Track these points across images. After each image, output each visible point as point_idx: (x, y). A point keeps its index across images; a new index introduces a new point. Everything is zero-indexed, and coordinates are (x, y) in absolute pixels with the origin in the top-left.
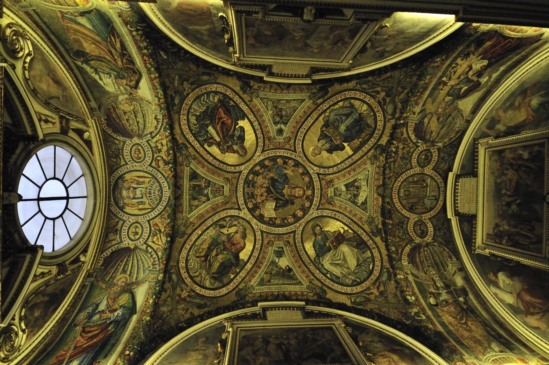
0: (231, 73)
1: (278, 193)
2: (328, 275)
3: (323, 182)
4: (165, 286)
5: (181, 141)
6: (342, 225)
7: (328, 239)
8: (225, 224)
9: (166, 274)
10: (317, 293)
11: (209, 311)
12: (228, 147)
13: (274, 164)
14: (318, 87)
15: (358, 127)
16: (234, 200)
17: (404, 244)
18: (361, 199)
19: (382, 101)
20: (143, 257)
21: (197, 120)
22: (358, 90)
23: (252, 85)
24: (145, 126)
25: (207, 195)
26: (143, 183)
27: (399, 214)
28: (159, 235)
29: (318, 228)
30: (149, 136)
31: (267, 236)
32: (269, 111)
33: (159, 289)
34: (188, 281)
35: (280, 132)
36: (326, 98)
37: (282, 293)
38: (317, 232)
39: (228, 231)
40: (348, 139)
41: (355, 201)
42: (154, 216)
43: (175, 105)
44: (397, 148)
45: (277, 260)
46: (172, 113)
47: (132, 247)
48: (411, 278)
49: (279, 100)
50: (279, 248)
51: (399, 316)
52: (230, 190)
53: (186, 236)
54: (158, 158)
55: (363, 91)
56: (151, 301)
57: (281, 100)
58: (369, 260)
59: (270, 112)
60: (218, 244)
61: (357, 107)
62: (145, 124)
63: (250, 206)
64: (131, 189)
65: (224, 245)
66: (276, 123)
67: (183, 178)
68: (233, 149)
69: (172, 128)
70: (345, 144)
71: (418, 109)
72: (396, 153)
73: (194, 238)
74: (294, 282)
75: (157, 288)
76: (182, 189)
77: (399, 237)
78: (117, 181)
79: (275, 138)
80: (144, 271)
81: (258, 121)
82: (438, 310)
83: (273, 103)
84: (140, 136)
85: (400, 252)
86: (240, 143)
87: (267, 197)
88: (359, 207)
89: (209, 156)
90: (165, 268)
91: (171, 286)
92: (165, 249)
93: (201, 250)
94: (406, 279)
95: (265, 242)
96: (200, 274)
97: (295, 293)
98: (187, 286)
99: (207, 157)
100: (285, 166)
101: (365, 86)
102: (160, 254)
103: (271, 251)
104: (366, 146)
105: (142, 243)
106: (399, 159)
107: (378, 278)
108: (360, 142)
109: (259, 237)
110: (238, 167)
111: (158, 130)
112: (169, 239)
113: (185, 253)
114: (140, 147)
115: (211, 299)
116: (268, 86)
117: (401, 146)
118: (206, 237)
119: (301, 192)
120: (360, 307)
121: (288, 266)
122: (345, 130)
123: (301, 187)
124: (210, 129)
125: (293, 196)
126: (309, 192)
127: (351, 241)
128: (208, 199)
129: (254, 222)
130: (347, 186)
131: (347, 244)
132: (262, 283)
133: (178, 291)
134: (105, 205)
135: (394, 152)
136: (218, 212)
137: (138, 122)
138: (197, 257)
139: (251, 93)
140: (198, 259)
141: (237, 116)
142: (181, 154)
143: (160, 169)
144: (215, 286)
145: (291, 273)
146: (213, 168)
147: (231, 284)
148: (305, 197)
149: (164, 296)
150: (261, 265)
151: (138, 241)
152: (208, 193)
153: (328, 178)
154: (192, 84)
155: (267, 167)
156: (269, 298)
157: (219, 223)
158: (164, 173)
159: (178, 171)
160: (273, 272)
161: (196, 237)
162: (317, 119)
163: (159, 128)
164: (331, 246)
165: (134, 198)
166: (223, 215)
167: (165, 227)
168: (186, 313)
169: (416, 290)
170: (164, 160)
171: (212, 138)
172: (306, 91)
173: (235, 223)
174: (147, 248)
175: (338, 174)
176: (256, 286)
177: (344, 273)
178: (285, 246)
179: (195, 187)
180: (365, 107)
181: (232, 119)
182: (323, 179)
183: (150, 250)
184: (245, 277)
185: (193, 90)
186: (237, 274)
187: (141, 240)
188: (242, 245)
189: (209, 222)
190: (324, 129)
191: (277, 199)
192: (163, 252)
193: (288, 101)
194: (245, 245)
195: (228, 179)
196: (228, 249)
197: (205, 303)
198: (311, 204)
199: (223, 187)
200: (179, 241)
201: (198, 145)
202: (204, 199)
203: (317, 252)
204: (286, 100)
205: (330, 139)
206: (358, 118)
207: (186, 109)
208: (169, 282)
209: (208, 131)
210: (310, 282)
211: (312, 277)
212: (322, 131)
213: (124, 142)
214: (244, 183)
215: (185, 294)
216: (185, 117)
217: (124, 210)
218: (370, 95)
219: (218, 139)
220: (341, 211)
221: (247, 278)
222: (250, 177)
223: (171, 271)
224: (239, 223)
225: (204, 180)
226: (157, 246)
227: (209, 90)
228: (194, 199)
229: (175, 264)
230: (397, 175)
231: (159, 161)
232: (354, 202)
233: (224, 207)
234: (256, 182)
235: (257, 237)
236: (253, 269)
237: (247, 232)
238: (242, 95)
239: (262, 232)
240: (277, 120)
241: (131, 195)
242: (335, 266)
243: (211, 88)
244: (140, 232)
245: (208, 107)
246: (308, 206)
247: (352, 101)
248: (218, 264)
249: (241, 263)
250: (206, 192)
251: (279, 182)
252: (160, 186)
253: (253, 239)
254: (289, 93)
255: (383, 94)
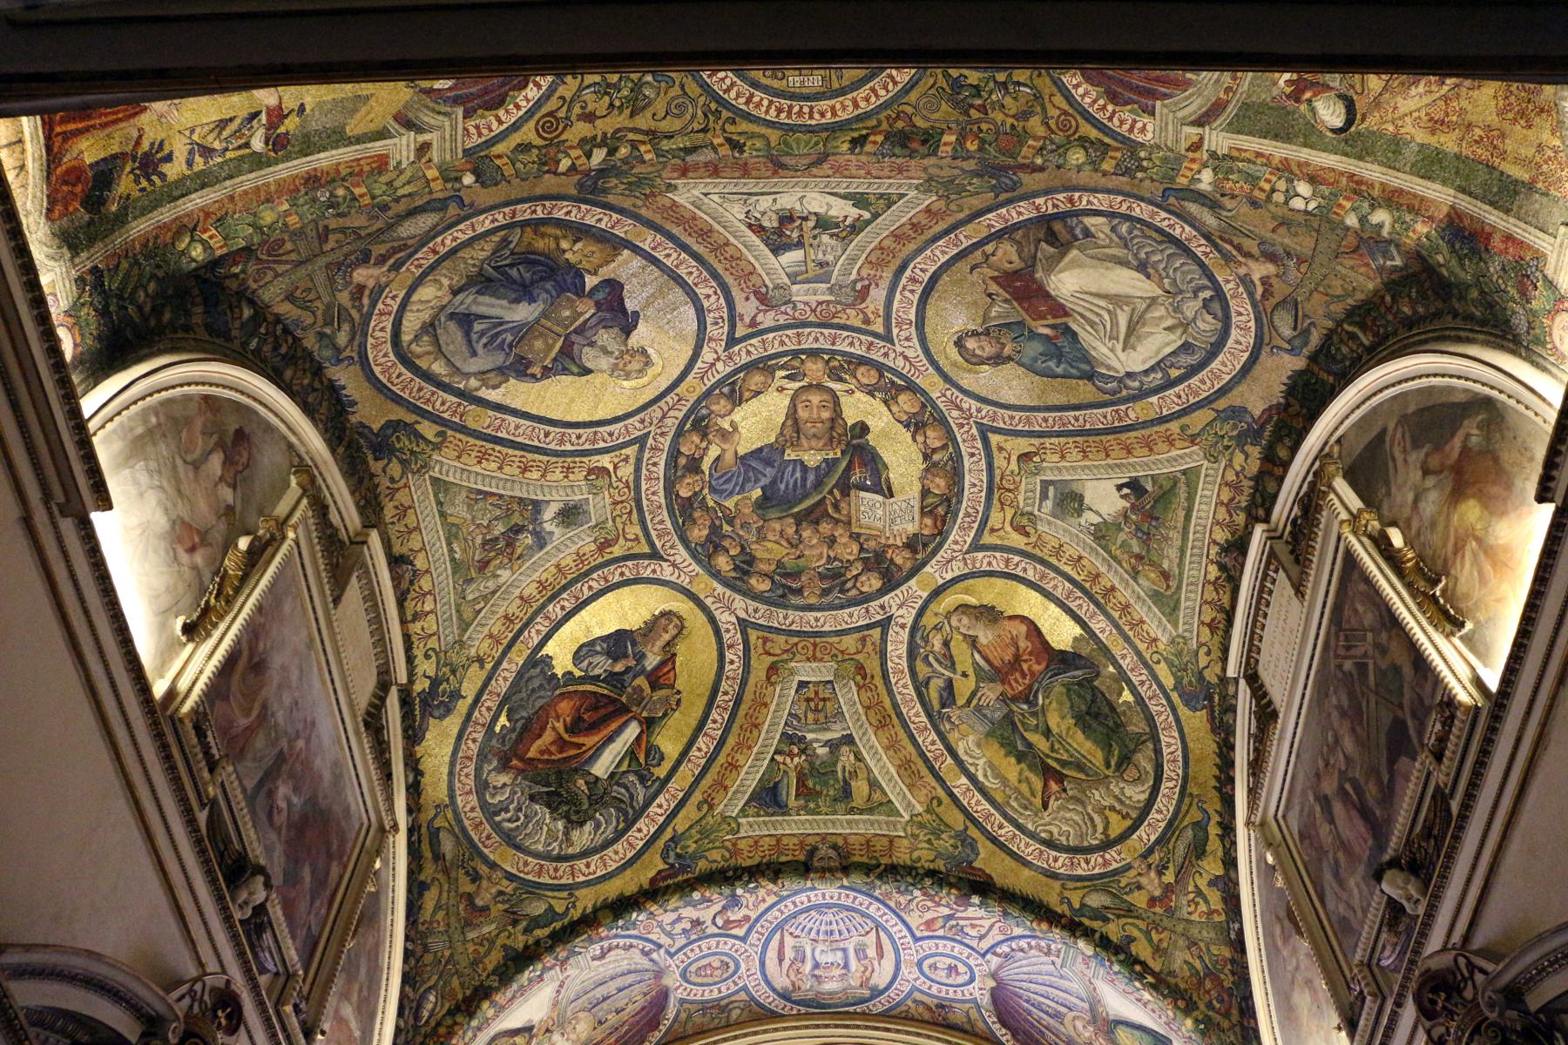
0: (411, 779)
1: (818, 484)
2: (1174, 373)
3: (767, 320)
4: (1114, 939)
5: (655, 864)
6: (964, 266)
7: (1021, 324)
8: (940, 682)
9: (1080, 924)
10: (1239, 435)
11: (1219, 824)
12: (654, 686)
13: (704, 505)
14: (376, 466)
15: (514, 272)
16: (850, 642)
17: (1059, 100)
18: (842, 210)
19: (392, 261)
20: (1025, 969)
21: (581, 824)
22: (363, 346)
23: (427, 683)
24: (630, 972)
25: (834, 746)
26: (798, 950)
27: (913, 96)
28: (962, 923)
29: (971, 344)
30: (655, 956)
31: (993, 530)
32: (502, 580)
33: (1121, 962)
34: (1115, 858)
35: (570, 514)
36: (410, 418)
37: (1214, 550)
38: (989, 350)
39: (964, 675)
40: (564, 279)
41: (853, 226)
42: (901, 926)
43: (551, 907)
44: (588, 145)
45: (1090, 518)
46: (576, 914)
47: (993, 984)
48: (1218, 140)
49: (456, 566)
50: (1044, 496)
51: (1368, 265)
52: (815, 659)
53: (973, 832)
54: (720, 922)
55: (360, 331)
56: (1146, 996)
57: (453, 560)
58: (1124, 228)
59: (505, 575)
60: (1009, 718)
61: (426, 316)
62: (623, 974)
63: (873, 583)
64: (817, 972)
65: (1015, 699)
66: (541, 541)
67: (779, 839)
68: (663, 664)
69: (622, 907)
70: (590, 281)
71: (402, 147)
72: (610, 143)
73: (980, 806)
74: (1183, 495)
75: (1116, 968)
76: (810, 840)
77: (1024, 115)
78: (794, 1002)
79: (600, 525)
80: (1062, 977)
81: (543, 606)
82: (1372, 122)
83: (470, 581)
84: (659, 974)
85: (1094, 134)
86: (634, 644)
87: (837, 521)
88: (876, 216)
89: (694, 752)
90: (1063, 928)
91: (1119, 917)
92: (1005, 914)
93: (1024, 788)
94: (1218, 161)
95: (1017, 540)
96: (1101, 810)
97: (1223, 510)
98: (1128, 867)
99: (698, 756)
100: (706, 465)
101: (342, 338)
102: (1018, 931)
103: (1054, 531)
104: (590, 221)
105: (980, 961)
106: (643, 121)
107: (1207, 237)
108: (575, 242)
109: (997, 562)
110: (726, 636)
111: (634, 942)
112: (976, 899)
113: (1027, 845)
114: (693, 968)
115: (1187, 800)
116: (416, 628)
117: (581, 129)
118: (981, 762)
119: (816, 399)
120: (1315, 339)
121: (1119, 488)
122: (532, 300)
123: (793, 399)
124: (602, 767)
125: (832, 428)
126: (815, 369)
127: (1035, 257)
128: (848, 740)
129: (935, 573)
130: (776, 251)
131: (1049, 270)
132: (1168, 604)
133: (1139, 900)
134: (867, 1028)
135: (612, 152)
136: (895, 706)
137: (620, 990)
138: (1045, 806)
139: (453, 672)
140: (1053, 804)
141: (541, 686)
142: (695, 857)
143: (754, 916)
144: (1149, 768)
145: (1149, 487)
146: (735, 728)
147: (1154, 709)
148: (832, 385)
149: (1142, 950)
150: (1105, 582)
151: (976, 970)
152: (826, 743)
153: (747, 308)
154: (475, 878)
155: (715, 530)
156: (1226, 600)
157: (936, 705)
158: (763, 907)
159: (757, 860)
160: (1136, 549)
161: (978, 796)
162: (499, 407)
163: (628, 941)
164: (1051, 321)
165: (846, 966)
166: (904, 688)
167: (939, 905)
168: (1206, 901)
169: (1278, 150)
170: (724, 908)
171: (631, 754)
172: (402, 497)
173: (937, 642)
174: (995, 954)
175: (729, 280)
176: (1176, 626)
177: (1169, 322)
178: (1038, 471)
179: (803, 791)
180: (427, 293)
181: (552, 704)
182: (753, 323)
183: (1005, 948)
184: (1139, 653)
185: (493, 866)
186: (1122, 676)
187: (972, 962)
188: (1023, 628)
189: (928, 740)
190: (536, 370)
191: (845, 488)
192: (1011, 922)
193: (452, 533)
194: (1023, 619)
195: (773, 669)
196: (1030, 687)
197: (1196, 824)
198: (863, 361)
199: (802, 685)
200: (988, 861)
201: (661, 799)
202: (846, 758)
203: (1074, 371)
204: (449, 544)
205: (574, 338)
206: (474, 290)
207: (556, 870)
208: (1106, 920)
209: (612, 775)
210: (1193, 440)
211: (1174, 426)
212: (547, 372)
213: (682, 1001)
214: (785, 607)
215: (1152, 881)
216: (581, 864)
217: (881, 987)
218: (373, 304)
219: (632, 731)
220: (897, 262)
221: (1142, 646)
222: (763, 586)
223: (1077, 906)
224: (936, 628)
225: (778, 757)
226: (995, 930)
227: (478, 814)
228: (847, 793)
229: (1057, 885)
230: (717, 113)
231: (727, 922)
232: (856, 228)
233: (878, 681)
234: (780, 564)
235: (995, 567)
236: (1116, 615)
237: (973, 601)
238: (470, 700)
239: (976, 547)
240: (529, 541)
241: (837, 972)
242: (1139, 338)
243: (473, 810)
244: (949, 961)
245: (532, 798)
246: (873, 372)
247: (406, 338)
248: (1080, 736)
249: (1085, 652)
250: (822, 751)
251: (774, 482)
252: (808, 910)
253: (1000, 582)
254: (423, 548)
255: (361, 275)
